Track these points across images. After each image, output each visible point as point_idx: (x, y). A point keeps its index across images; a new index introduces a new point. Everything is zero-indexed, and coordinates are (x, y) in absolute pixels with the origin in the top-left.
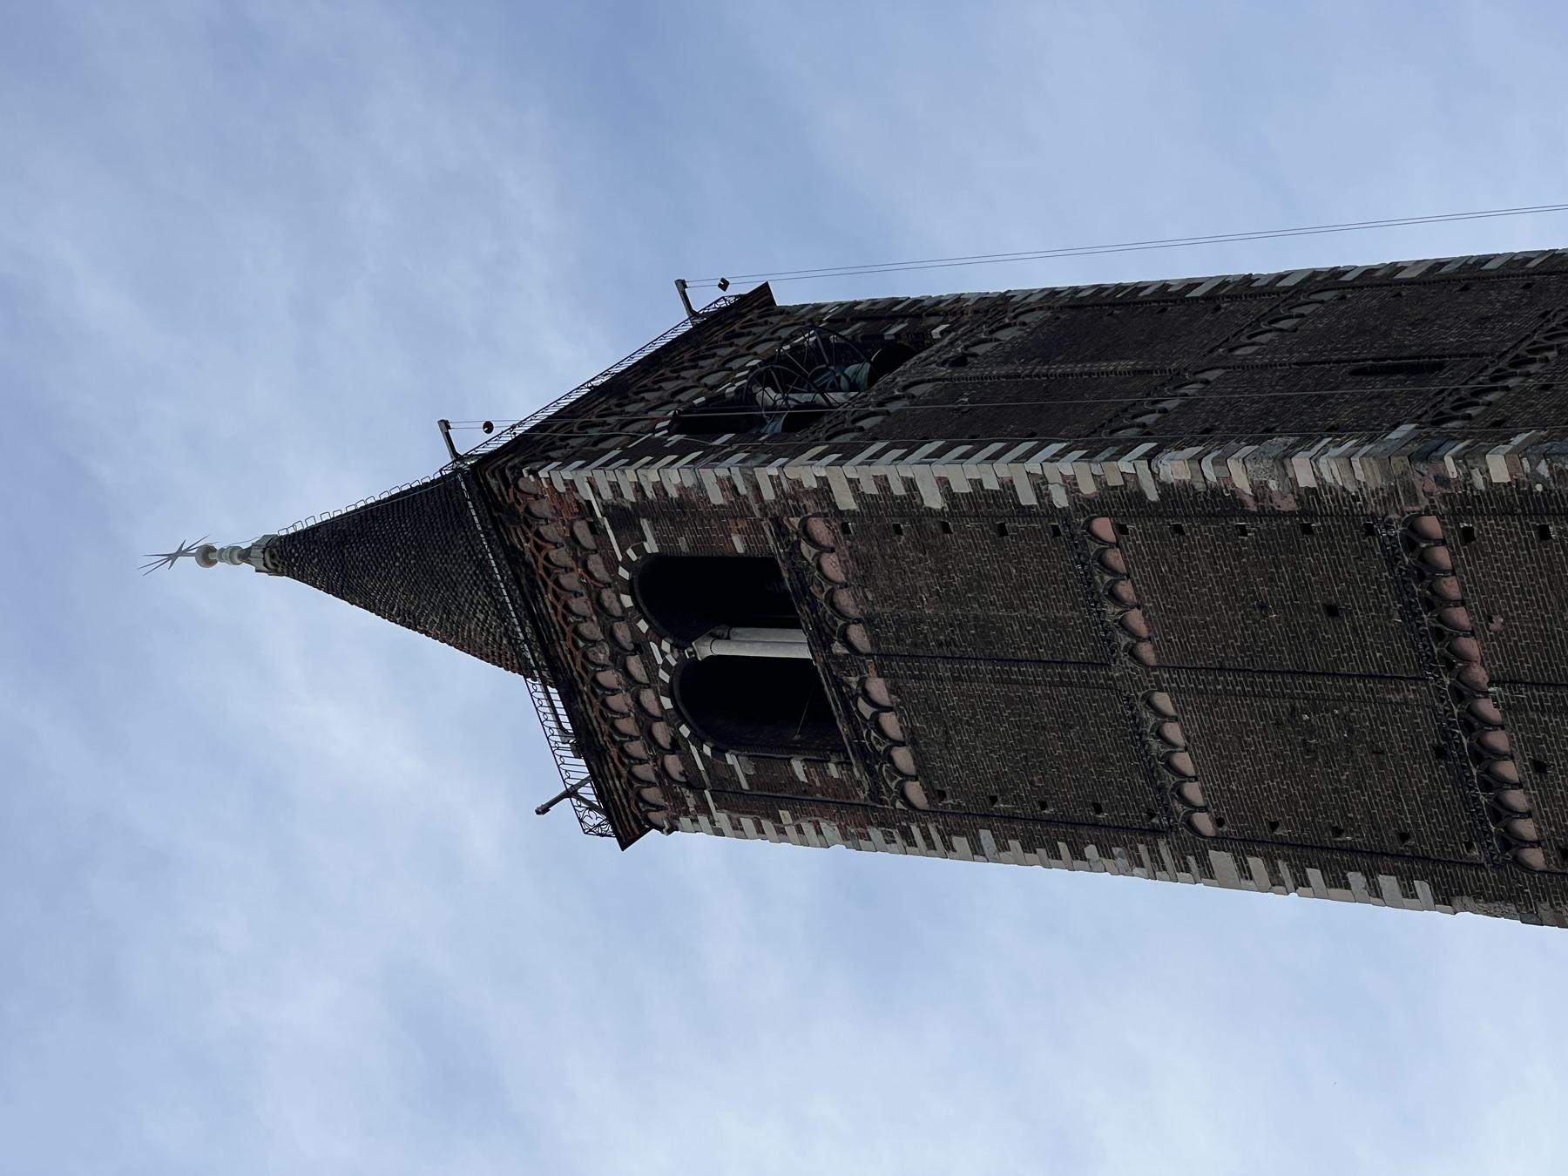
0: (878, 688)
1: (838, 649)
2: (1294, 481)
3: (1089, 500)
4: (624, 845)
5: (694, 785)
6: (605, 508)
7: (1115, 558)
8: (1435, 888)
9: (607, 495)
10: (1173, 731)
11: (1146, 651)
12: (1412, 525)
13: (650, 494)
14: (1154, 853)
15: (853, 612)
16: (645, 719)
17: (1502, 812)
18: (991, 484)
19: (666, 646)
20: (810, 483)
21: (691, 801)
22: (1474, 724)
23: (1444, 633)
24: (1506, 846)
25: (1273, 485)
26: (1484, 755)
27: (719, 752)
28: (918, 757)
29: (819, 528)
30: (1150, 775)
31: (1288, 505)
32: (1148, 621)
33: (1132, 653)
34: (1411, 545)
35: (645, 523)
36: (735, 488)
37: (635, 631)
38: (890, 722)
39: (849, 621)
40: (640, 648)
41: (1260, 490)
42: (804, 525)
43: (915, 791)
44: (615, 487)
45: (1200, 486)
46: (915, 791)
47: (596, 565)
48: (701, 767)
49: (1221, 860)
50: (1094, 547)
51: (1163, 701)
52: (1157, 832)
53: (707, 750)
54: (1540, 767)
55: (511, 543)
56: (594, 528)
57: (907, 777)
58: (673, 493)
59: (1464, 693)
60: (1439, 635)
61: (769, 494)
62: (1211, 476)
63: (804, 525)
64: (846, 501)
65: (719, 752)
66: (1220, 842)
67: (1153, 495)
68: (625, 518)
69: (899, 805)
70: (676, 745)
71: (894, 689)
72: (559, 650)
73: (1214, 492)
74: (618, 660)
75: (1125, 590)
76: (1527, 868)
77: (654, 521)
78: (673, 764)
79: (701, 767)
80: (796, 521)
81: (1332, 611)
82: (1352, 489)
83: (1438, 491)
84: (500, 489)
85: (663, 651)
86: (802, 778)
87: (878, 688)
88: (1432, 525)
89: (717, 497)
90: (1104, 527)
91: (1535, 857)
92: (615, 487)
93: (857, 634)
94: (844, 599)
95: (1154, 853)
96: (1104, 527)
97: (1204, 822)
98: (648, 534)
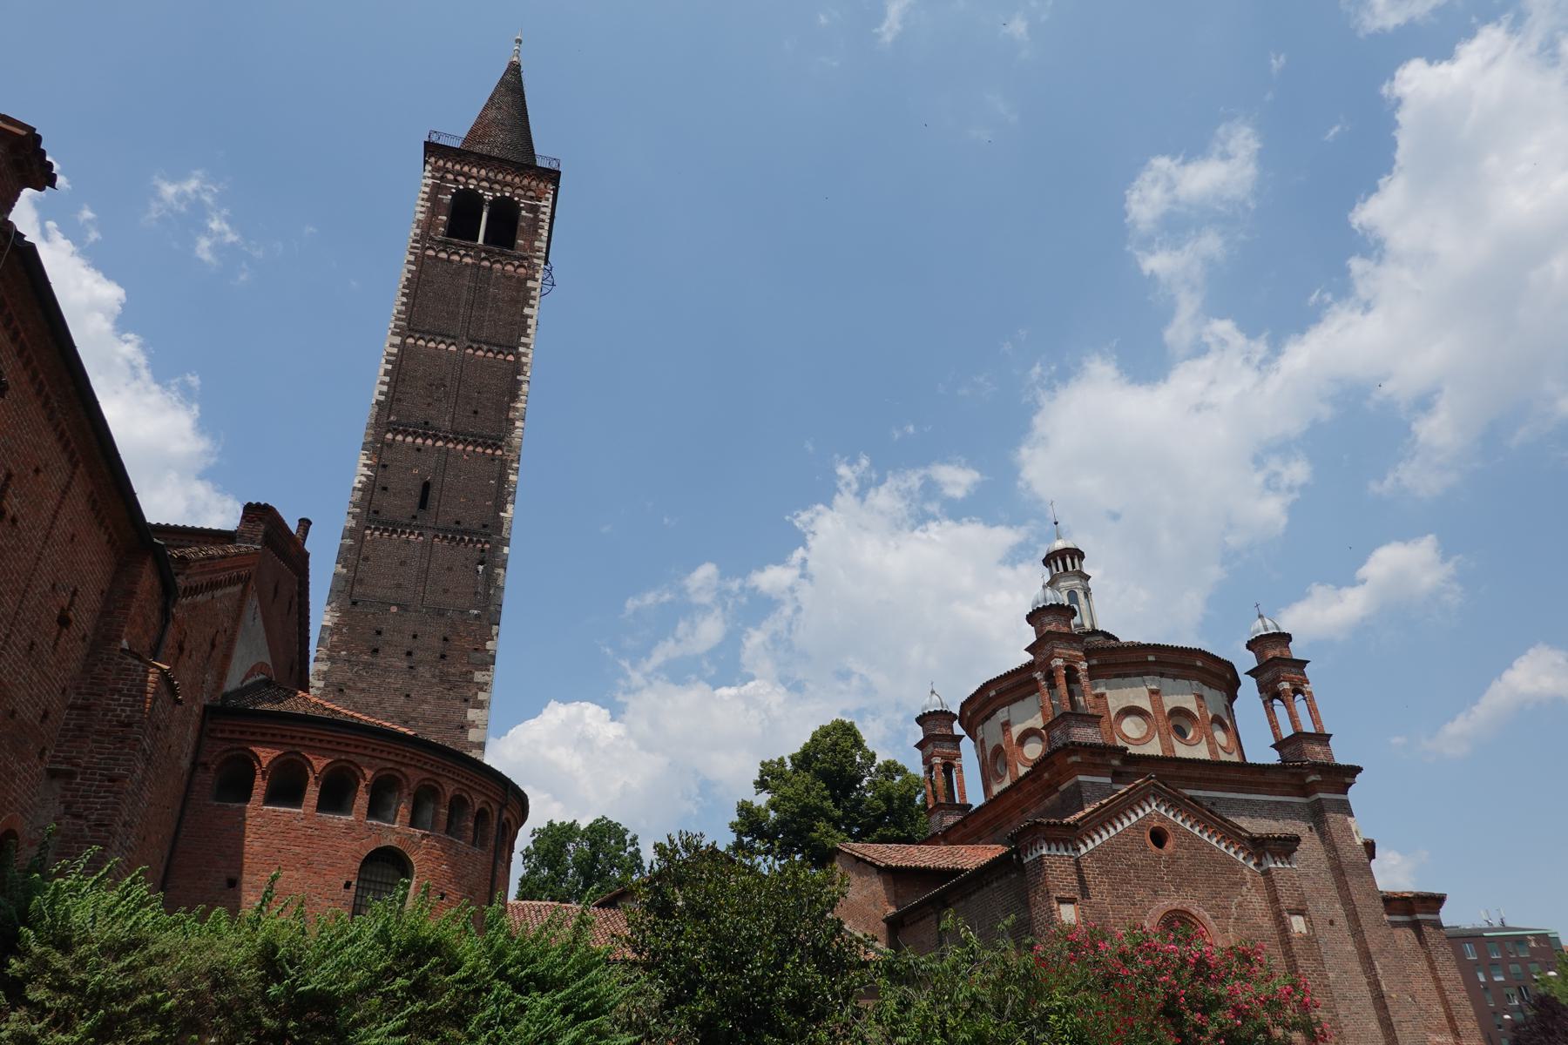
0: (468, 260)
1: (483, 255)
2: (518, 420)
3: (520, 358)
4: (425, 142)
5: (442, 178)
6: (539, 207)
7: (501, 356)
8: (382, 402)
9: (543, 209)
10: (442, 346)
11: (470, 351)
12: (500, 448)
13: (541, 223)
14: (402, 320)
15: (494, 266)
16: (468, 176)
17: (406, 433)
18: (529, 331)
19: (491, 198)
20: (537, 276)
21: (437, 174)
22: (436, 438)
23: (466, 442)
24: (395, 429)
25: (517, 414)
26: (425, 436)
27: (452, 194)
28: (442, 259)
29: (522, 270)
30: (429, 333)
31: (511, 415)
32: (479, 356)
33: (471, 347)
34: (494, 444)
35: (531, 215)
36: (539, 251)
37: (497, 191)
38: (456, 258)
39: (492, 263)
40: (491, 189)
41: (517, 409)
42: (524, 267)
43: (431, 253)
44: (544, 213)
45: (520, 392)
46: (431, 253)
47: (519, 191)
48: (448, 185)
49: (397, 340)
50: (506, 352)
51: (453, 348)
52: (409, 324)
53: (454, 191)
54: (419, 450)
56: (531, 198)
57: (437, 253)
58: (540, 231)
59: (447, 440)
60: (466, 440)
61: (536, 261)
62: (522, 397)
63: (524, 267)
64: (530, 284)
65: (452, 194)
66: (403, 342)
67: (518, 377)
68: (535, 210)
69: (427, 245)
70: (456, 180)
71: (467, 264)
73: (518, 396)
74: (487, 179)
75: (490, 355)
76: (386, 433)
77: (532, 219)
78: (450, 177)
79: (448, 185)
80: (526, 264)
81: (476, 412)
82: (513, 435)
83: (510, 459)
85: (488, 196)
86: (440, 217)
87: (468, 260)
88: (499, 452)
89: (537, 244)
90: (511, 358)
91: (389, 436)
92: (544, 213)
93: (486, 263)
94: (498, 266)
95: (402, 320)
96: (511, 358)
97: (411, 341)
98: (527, 214)
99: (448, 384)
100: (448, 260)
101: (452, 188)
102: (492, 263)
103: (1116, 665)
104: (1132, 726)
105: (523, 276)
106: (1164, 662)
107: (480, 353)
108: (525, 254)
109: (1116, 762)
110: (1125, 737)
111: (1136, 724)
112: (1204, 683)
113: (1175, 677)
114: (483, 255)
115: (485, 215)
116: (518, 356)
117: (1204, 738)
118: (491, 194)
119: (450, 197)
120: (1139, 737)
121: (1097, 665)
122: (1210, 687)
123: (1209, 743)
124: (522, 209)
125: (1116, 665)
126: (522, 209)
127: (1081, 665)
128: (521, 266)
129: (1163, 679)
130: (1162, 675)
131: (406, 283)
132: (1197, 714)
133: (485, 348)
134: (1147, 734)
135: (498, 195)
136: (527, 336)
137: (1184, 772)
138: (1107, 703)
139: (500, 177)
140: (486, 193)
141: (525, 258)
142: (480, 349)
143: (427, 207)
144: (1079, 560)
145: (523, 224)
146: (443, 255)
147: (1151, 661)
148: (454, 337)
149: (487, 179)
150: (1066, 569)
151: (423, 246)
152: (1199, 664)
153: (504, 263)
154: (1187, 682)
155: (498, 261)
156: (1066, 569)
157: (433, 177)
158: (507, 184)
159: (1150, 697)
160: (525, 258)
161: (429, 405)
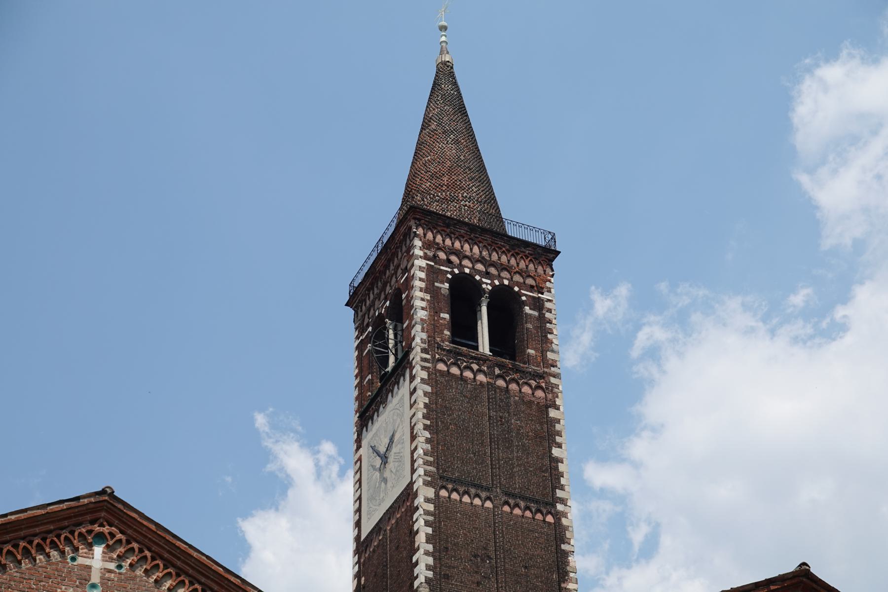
0: (481, 378)
3: (560, 519)
11: (506, 508)
16: (461, 256)
27: (448, 281)
29: (540, 393)
38: (468, 374)
40: (487, 274)
48: (442, 268)
50: (545, 512)
51: (488, 504)
53: (449, 276)
55: (530, 247)
58: (549, 336)
66: (437, 494)
69: (437, 356)
72: (489, 236)
74: (482, 260)
79: (442, 268)
80: (543, 385)
84: (548, 256)
86: (442, 315)
96: (550, 519)
99: (493, 556)
100: (462, 378)
101: (447, 272)
102: (508, 383)
105: (543, 402)
107: (517, 511)
108: (540, 370)
114: (497, 371)
115: (484, 309)
116: (558, 516)
118: (489, 282)
119: (447, 285)
124: (524, 303)
126: (524, 303)
128: (539, 387)
131: (425, 412)
133: (522, 504)
135: (497, 282)
136: (562, 488)
139: (495, 257)
140: (484, 280)
141: (541, 376)
142: (517, 505)
143: (428, 300)
145: (530, 326)
146: (455, 370)
148: (487, 489)
149: (482, 260)
151: (433, 357)
153: (521, 382)
155: (513, 380)
157: (426, 257)
158: (507, 268)
160: (541, 376)
161: (478, 584)
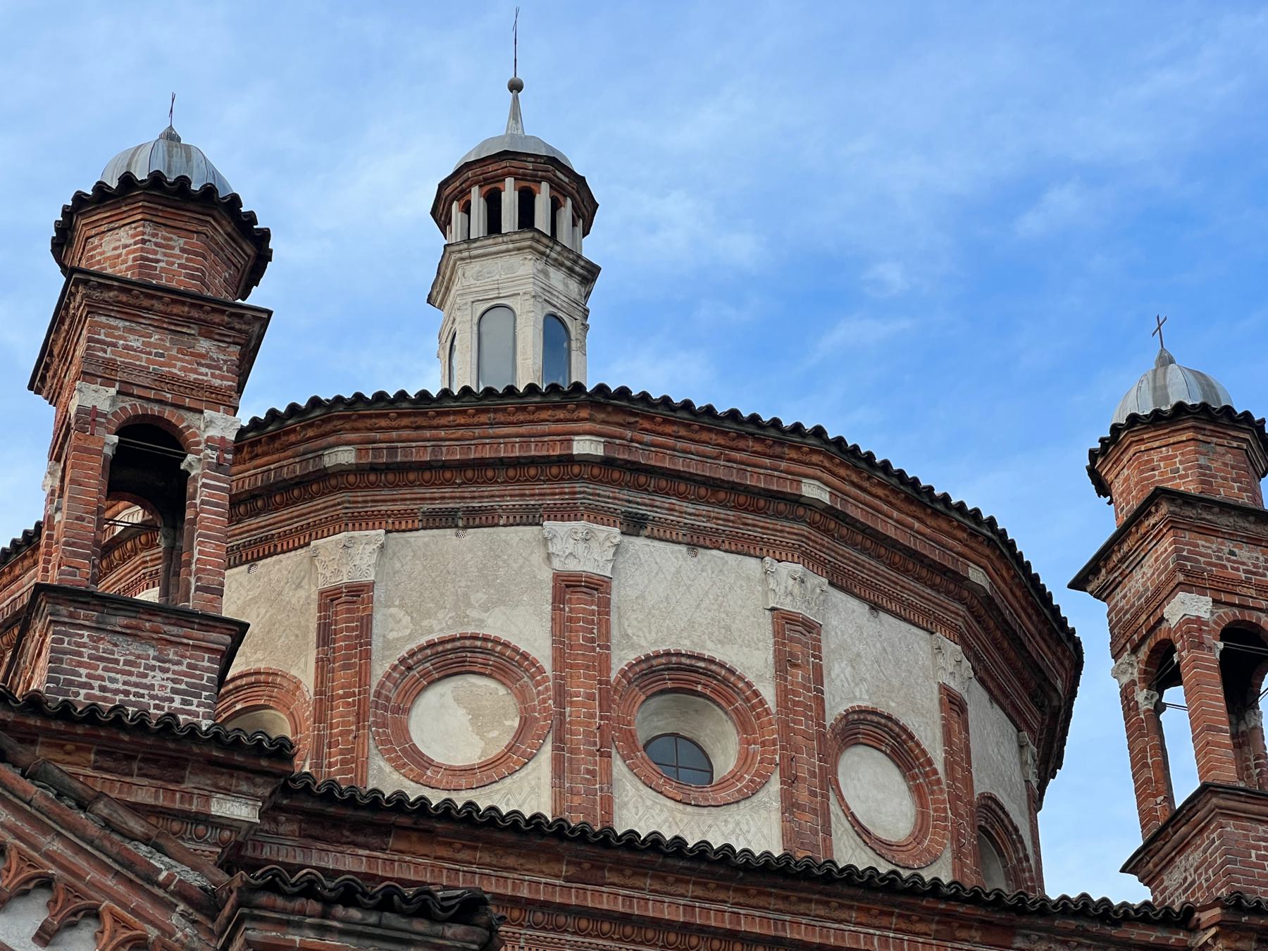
103: (435, 471)
104: (459, 718)
106: (650, 471)
109: (241, 811)
110: (415, 761)
111: (476, 716)
112: (841, 581)
113: (697, 540)
117: (775, 785)
120: (459, 761)
121: (358, 470)
122: (875, 607)
123: (790, 806)
125: (435, 471)
127: (209, 424)
129: (639, 544)
130: (634, 525)
132: (769, 693)
134: (511, 748)
137: (607, 899)
138: (366, 625)
144: (555, 206)
147: (586, 460)
150: (494, 226)
152: (812, 490)
154: (752, 563)
156: (494, 226)
159: (558, 600)
